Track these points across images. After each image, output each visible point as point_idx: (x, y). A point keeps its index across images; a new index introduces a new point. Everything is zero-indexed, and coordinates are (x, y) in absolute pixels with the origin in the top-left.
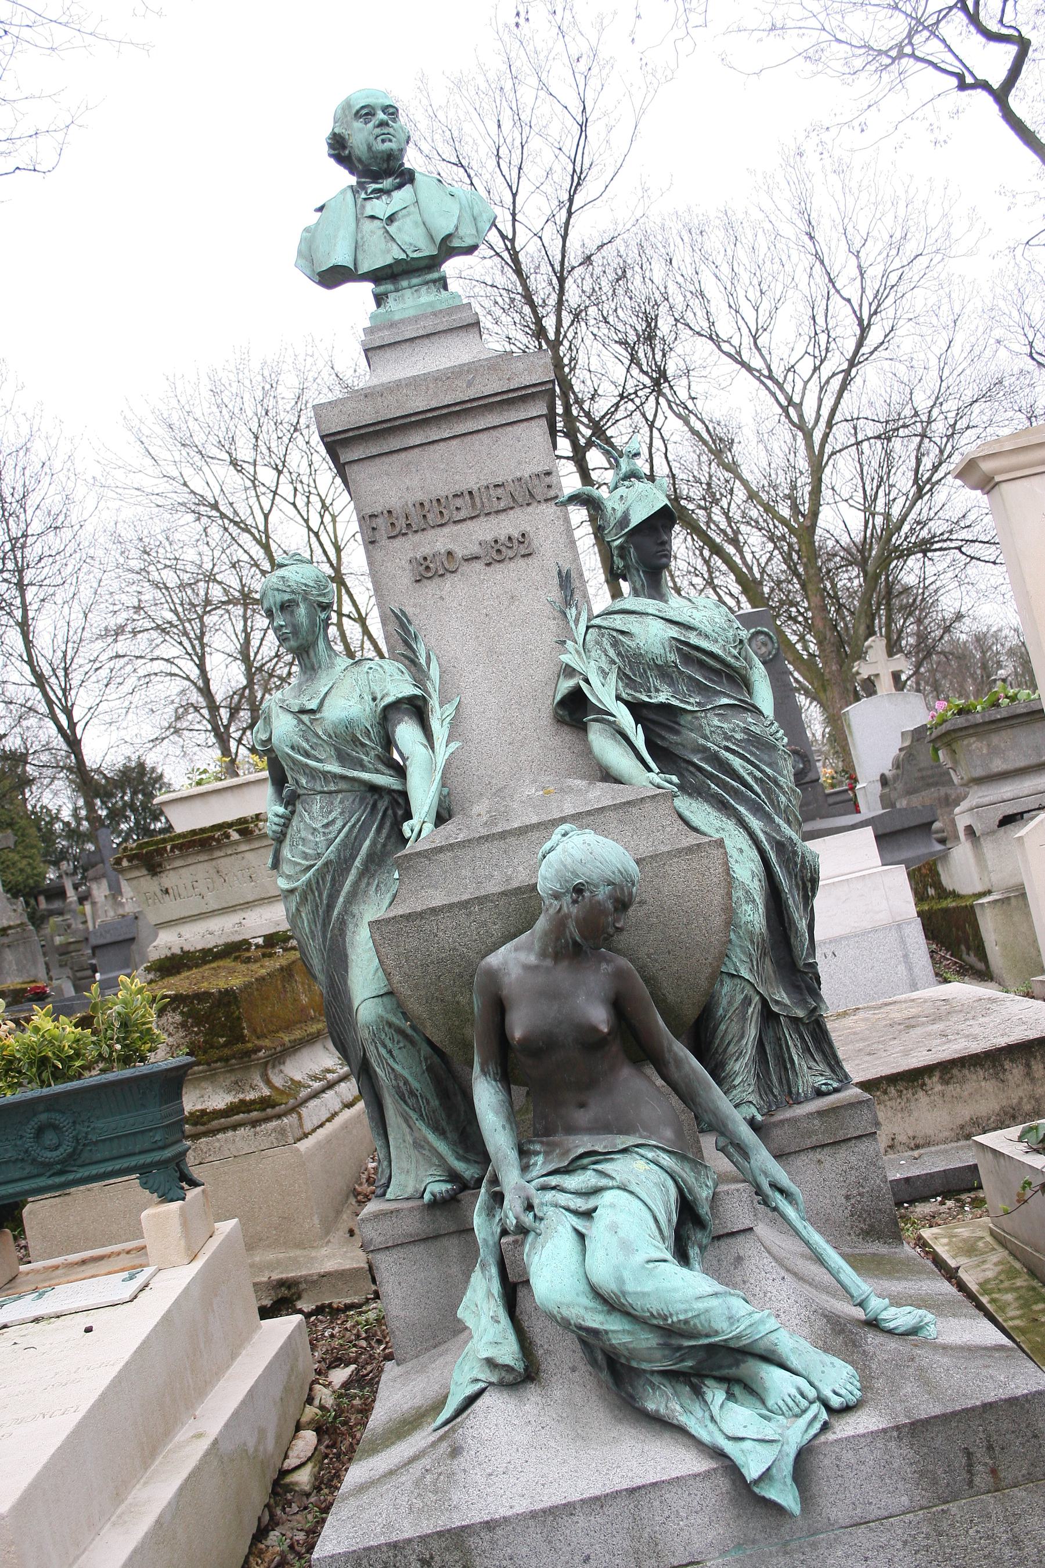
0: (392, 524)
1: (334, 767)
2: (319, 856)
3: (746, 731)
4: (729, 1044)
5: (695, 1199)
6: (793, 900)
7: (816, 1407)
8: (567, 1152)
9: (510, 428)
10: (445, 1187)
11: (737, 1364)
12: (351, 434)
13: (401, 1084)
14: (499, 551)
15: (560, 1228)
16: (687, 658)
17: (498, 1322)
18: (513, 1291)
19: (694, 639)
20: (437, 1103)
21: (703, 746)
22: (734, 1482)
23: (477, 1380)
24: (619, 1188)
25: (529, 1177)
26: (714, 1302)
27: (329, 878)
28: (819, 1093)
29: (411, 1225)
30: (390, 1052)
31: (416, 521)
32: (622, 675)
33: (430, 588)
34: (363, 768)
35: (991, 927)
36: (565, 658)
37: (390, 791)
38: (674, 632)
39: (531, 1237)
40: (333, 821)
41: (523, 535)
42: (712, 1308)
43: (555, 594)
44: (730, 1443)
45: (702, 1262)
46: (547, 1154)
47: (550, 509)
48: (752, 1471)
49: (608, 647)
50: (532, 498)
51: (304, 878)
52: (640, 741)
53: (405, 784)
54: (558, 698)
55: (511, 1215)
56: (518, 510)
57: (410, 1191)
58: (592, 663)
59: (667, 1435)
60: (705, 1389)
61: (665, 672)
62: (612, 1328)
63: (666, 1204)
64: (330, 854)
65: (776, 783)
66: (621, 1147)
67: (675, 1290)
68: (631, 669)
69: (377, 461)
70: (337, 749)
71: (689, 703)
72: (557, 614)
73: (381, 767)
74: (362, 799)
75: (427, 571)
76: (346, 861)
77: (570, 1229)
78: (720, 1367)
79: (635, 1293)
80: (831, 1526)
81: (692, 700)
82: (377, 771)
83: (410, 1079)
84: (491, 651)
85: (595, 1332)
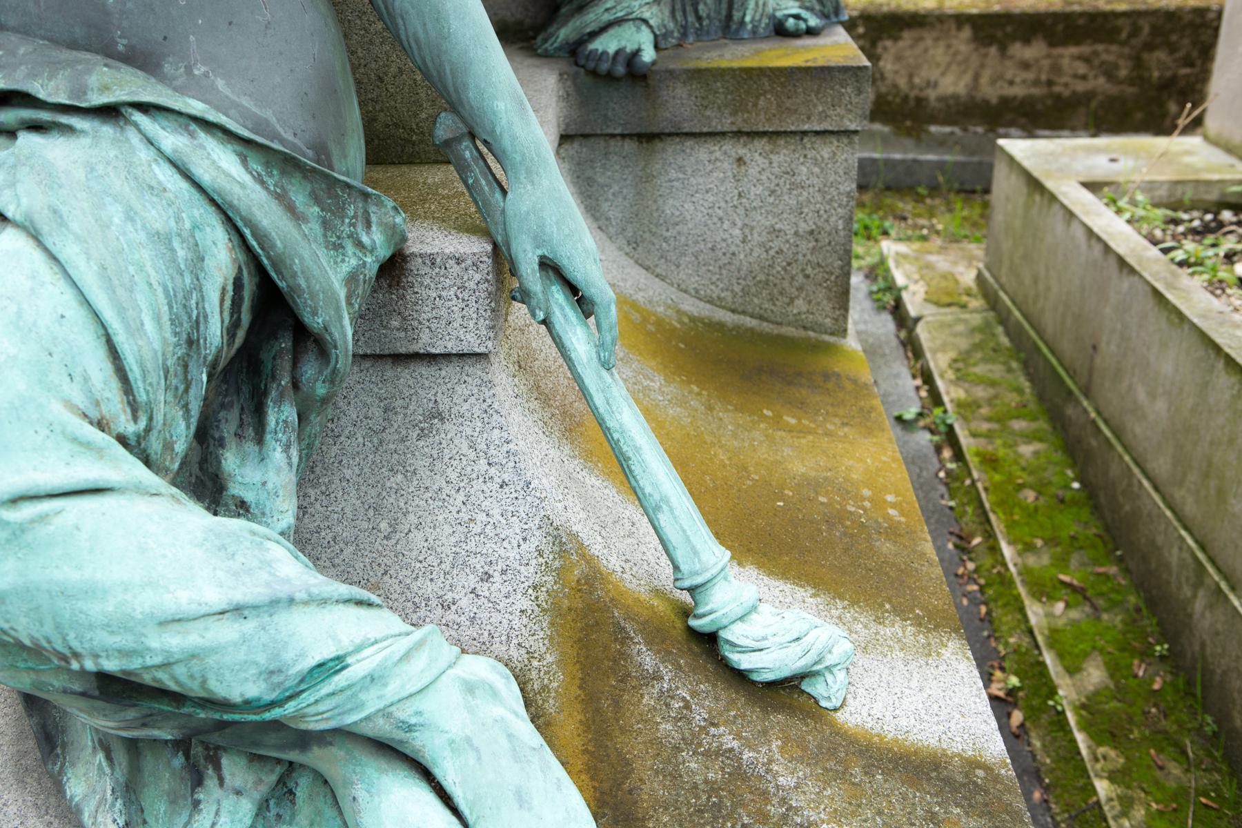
26: (226, 632)
28: (780, 31)
42: (214, 650)
66: (97, 100)
67: (91, 591)
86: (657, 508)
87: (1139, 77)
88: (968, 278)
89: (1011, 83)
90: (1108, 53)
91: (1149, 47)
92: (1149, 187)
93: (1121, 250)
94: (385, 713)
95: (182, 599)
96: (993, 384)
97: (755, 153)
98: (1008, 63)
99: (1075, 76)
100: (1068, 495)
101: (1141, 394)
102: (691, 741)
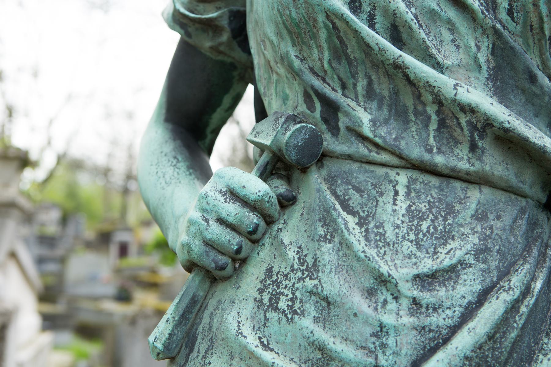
40: (451, 273)
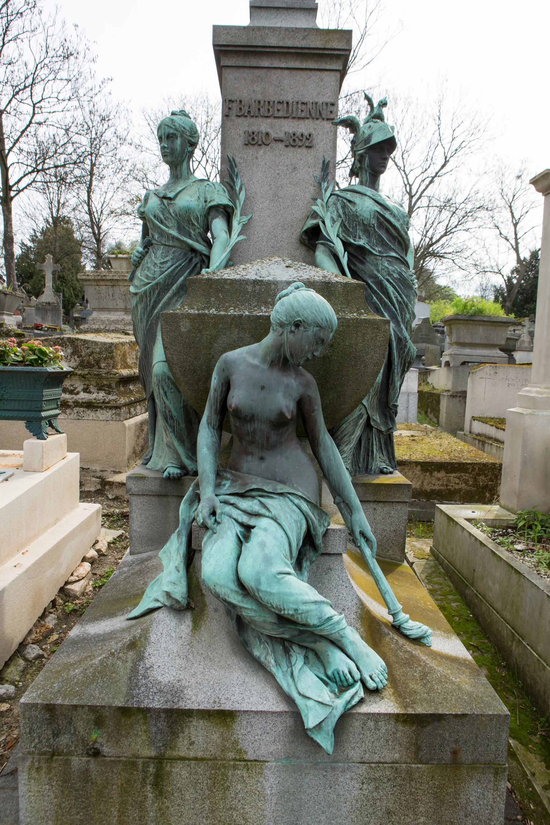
0: (240, 109)
1: (174, 232)
2: (154, 278)
3: (400, 274)
4: (344, 436)
5: (316, 534)
6: (397, 369)
7: (359, 685)
8: (245, 485)
9: (318, 73)
10: (177, 471)
11: (315, 642)
12: (230, 49)
13: (167, 411)
14: (294, 140)
15: (229, 533)
16: (380, 225)
17: (178, 571)
18: (192, 556)
19: (387, 215)
20: (184, 426)
21: (376, 275)
22: (296, 722)
23: (157, 600)
24: (272, 518)
25: (218, 493)
26: (313, 607)
27: (157, 292)
28: (382, 472)
29: (154, 486)
30: (165, 393)
31: (254, 111)
32: (343, 225)
33: (251, 150)
34: (190, 237)
35: (444, 404)
36: (314, 208)
37: (201, 254)
38: (378, 208)
39: (209, 533)
40: (167, 262)
41: (310, 135)
42: (311, 611)
43: (318, 173)
44: (300, 697)
45: (309, 571)
46: (233, 481)
47: (328, 125)
48: (311, 722)
49: (340, 207)
50: (319, 116)
51: (143, 289)
52: (344, 261)
53: (210, 252)
54: (305, 228)
55: (200, 515)
56: (310, 120)
57: (159, 467)
58: (329, 213)
59: (261, 673)
60: (292, 653)
61: (367, 230)
62: (245, 606)
63: (298, 534)
64: (160, 279)
65: (407, 306)
66: (279, 491)
67: (291, 595)
68: (349, 223)
69: (241, 70)
70: (178, 223)
71: (374, 250)
72: (316, 184)
73: (200, 239)
74: (185, 254)
75: (254, 141)
76: (168, 285)
77: (235, 535)
78: (304, 641)
79: (266, 592)
80: (348, 759)
81: (377, 249)
82: (197, 241)
83: (172, 410)
84: (275, 194)
85: (234, 606)
86: (385, 593)
87: (476, 484)
88: (428, 550)
89: (434, 485)
90: (466, 476)
91: (479, 475)
92: (486, 521)
93: (481, 539)
94: (338, 632)
95: (306, 598)
96: (440, 584)
97: (379, 507)
98: (433, 478)
99: (455, 483)
100: (469, 619)
101: (490, 583)
102: (400, 648)
